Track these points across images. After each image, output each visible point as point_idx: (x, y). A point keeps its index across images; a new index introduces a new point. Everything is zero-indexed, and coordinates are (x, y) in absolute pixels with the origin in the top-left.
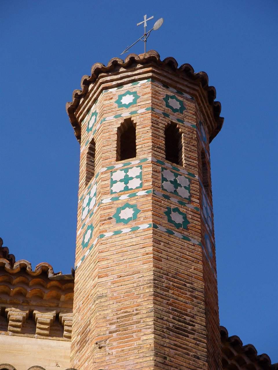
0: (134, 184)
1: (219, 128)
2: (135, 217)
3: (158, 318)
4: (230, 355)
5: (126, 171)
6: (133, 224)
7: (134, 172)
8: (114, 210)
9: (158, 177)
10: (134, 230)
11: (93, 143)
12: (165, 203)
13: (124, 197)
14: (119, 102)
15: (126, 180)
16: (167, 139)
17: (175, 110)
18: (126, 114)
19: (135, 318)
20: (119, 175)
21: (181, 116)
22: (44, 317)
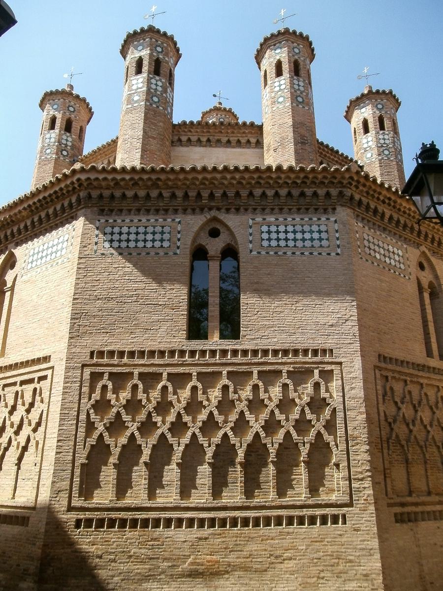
0: (283, 87)
3: (295, 139)
4: (320, 148)
7: (283, 82)
9: (292, 84)
11: (266, 71)
12: (295, 94)
15: (280, 86)
16: (294, 67)
18: (278, 58)
20: (277, 84)
22: (253, 140)
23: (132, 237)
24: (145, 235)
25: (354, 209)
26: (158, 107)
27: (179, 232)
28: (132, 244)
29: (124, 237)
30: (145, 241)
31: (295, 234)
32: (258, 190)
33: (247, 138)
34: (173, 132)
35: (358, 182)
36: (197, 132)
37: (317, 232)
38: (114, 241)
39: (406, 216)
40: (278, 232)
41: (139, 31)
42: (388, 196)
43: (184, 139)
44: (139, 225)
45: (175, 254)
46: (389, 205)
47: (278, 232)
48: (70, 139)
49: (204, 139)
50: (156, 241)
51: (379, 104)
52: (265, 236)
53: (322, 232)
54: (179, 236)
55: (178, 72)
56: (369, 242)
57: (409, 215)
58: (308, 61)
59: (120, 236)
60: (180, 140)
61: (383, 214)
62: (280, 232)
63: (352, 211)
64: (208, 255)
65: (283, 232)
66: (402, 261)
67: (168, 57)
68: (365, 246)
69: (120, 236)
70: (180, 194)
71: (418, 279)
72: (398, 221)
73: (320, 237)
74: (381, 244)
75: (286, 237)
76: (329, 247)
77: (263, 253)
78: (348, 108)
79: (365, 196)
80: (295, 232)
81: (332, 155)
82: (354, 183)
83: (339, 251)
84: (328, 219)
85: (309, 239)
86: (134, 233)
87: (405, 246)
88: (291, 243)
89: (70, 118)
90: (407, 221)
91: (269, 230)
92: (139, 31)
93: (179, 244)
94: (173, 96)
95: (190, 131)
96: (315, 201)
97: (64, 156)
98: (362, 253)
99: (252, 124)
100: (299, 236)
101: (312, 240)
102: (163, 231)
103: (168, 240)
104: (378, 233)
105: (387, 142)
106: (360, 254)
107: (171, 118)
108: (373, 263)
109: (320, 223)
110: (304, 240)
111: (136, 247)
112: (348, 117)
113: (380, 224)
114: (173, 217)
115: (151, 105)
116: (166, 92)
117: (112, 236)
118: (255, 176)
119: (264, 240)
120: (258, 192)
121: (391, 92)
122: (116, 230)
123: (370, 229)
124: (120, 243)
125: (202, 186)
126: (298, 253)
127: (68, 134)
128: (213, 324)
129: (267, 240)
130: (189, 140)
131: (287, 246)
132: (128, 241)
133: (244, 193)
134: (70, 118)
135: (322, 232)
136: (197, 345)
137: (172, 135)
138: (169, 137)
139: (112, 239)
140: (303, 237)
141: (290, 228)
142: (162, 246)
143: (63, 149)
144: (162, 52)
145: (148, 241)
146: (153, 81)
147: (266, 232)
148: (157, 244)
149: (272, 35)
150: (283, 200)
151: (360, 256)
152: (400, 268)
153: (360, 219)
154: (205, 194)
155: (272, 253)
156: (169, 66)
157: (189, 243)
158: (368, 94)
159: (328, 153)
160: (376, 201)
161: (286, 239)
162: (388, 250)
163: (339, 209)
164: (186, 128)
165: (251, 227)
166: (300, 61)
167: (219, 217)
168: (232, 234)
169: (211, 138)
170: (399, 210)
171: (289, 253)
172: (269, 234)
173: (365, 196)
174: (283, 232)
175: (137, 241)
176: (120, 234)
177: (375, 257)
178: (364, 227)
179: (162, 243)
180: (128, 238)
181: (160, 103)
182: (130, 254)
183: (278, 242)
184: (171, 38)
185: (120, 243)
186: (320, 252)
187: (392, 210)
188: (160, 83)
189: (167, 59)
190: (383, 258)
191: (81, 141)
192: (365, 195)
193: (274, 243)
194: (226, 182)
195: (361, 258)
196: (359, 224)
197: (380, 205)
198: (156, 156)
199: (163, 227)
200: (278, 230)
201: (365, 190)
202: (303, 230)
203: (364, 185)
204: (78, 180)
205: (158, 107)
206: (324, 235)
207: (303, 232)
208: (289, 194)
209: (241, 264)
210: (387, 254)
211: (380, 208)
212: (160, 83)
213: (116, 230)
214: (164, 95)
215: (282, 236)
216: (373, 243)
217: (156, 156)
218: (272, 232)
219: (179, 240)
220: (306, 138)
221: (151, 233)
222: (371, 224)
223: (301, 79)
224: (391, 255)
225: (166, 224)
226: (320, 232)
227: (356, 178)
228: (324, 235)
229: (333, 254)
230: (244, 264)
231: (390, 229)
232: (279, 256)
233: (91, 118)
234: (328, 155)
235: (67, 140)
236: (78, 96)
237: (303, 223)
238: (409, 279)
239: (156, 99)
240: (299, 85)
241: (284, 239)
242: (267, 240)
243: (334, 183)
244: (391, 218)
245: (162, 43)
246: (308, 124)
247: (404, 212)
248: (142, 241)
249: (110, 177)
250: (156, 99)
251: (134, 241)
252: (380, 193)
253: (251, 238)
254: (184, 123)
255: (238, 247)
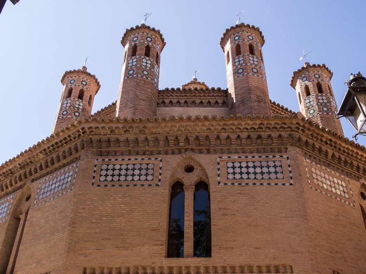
1: (264, 43)
2: (243, 72)
4: (273, 107)
5: (239, 59)
6: (243, 73)
7: (241, 59)
8: (237, 71)
10: (243, 75)
13: (239, 66)
14: (234, 39)
15: (239, 61)
16: (249, 48)
17: (251, 39)
18: (237, 42)
19: (246, 99)
21: (253, 41)
22: (220, 101)
23: (123, 172)
24: (133, 171)
25: (302, 149)
26: (147, 78)
27: (161, 168)
28: (123, 178)
29: (117, 172)
30: (133, 175)
31: (255, 169)
32: (223, 134)
33: (215, 100)
34: (159, 96)
35: (304, 127)
36: (177, 96)
37: (273, 167)
38: (108, 175)
39: (346, 154)
40: (241, 167)
41: (135, 28)
42: (329, 138)
43: (167, 101)
44: (129, 163)
45: (157, 185)
46: (331, 145)
47: (241, 167)
48: (81, 104)
49: (182, 101)
50: (142, 175)
51: (316, 74)
52: (231, 170)
53: (277, 166)
54: (160, 171)
55: (162, 55)
56: (317, 175)
57: (348, 154)
58: (260, 45)
59: (113, 171)
60: (164, 102)
61: (327, 152)
62: (243, 167)
63: (301, 150)
64: (184, 186)
65: (245, 167)
66: (346, 191)
67: (155, 44)
68: (314, 178)
69: (113, 171)
70: (161, 138)
71: (360, 204)
72: (340, 158)
73: (276, 171)
74: (327, 176)
75: (248, 171)
76: (283, 178)
77: (229, 184)
78: (293, 78)
79: (310, 139)
80: (254, 167)
81: (282, 112)
82: (301, 128)
83: (292, 181)
84: (281, 156)
85: (267, 173)
86: (125, 169)
87: (347, 179)
88: (252, 176)
89: (83, 89)
90: (347, 158)
91: (233, 166)
92: (135, 28)
93: (160, 177)
94: (159, 71)
95: (172, 96)
96: (270, 141)
97: (76, 116)
98: (312, 183)
99: (219, 89)
100: (258, 170)
101: (269, 173)
102: (147, 167)
103: (151, 175)
104: (324, 168)
105: (325, 101)
106: (310, 184)
107: (157, 86)
108: (321, 192)
109: (275, 160)
110: (262, 173)
111: (126, 180)
112: (293, 85)
113: (325, 161)
114: (156, 156)
115: (142, 76)
116: (153, 68)
117: (107, 171)
118: (221, 124)
119: (229, 173)
120: (224, 135)
121: (324, 66)
122: (111, 167)
123: (316, 164)
124: (113, 177)
125: (179, 132)
126: (258, 184)
127: (80, 101)
128: (188, 244)
129: (232, 173)
130: (171, 102)
131: (248, 178)
132: (120, 175)
133: (213, 137)
134: (83, 89)
135: (277, 166)
136: (175, 262)
137: (158, 99)
138: (155, 100)
139: (107, 174)
140: (262, 171)
141: (251, 164)
142: (146, 179)
143: (76, 111)
144: (151, 41)
145: (135, 175)
146: (144, 60)
147: (231, 167)
148: (143, 178)
149: (232, 28)
150: (244, 142)
151: (310, 186)
152: (345, 197)
153: (308, 156)
154: (182, 139)
155: (236, 184)
156: (156, 50)
157: (169, 176)
158: (306, 68)
159: (279, 110)
160: (320, 142)
161: (248, 173)
162: (333, 182)
163: (290, 148)
164: (168, 93)
165: (218, 163)
166: (254, 45)
167: (192, 156)
168: (203, 170)
169: (188, 100)
170: (339, 149)
171: (251, 184)
172: (234, 169)
173: (310, 139)
174: (245, 167)
175: (126, 175)
176: (114, 170)
177: (323, 187)
178: (311, 163)
179: (146, 177)
180: (120, 173)
181: (149, 75)
182: (121, 186)
183: (241, 175)
184: (158, 32)
185: (113, 177)
186: (276, 183)
187: (333, 150)
188: (149, 62)
189: (154, 45)
190: (329, 188)
191: (90, 106)
192: (310, 137)
193: (238, 176)
194: (198, 129)
195: (311, 188)
196: (307, 160)
197: (324, 145)
198: (145, 113)
199: (148, 164)
200: (240, 165)
201: (310, 133)
202: (261, 165)
203: (309, 130)
204: (83, 129)
205: (147, 78)
206: (279, 169)
207: (262, 167)
208: (249, 137)
209: (211, 194)
210: (332, 185)
211: (324, 148)
212: (149, 62)
213: (111, 167)
214: (152, 70)
215: (244, 170)
216: (320, 175)
217: (145, 113)
218: (236, 167)
219: (160, 174)
220: (261, 98)
221: (138, 169)
222: (317, 161)
223: (255, 57)
224: (337, 186)
225: (150, 162)
226: (275, 167)
227: (302, 124)
228: (279, 169)
229: (287, 184)
230: (214, 193)
231: (333, 165)
232: (243, 186)
233: (98, 90)
234: (279, 112)
235: (79, 105)
236: (89, 74)
237: (261, 159)
238: (354, 206)
239: (145, 73)
240: (253, 61)
241: (246, 173)
242: (232, 173)
243: (284, 128)
244: (333, 156)
245: (152, 36)
246: (262, 88)
247: (344, 151)
248: (131, 175)
249: (107, 126)
250: (145, 73)
251: (124, 175)
252: (322, 136)
253: (219, 172)
254: (167, 89)
255: (209, 180)
